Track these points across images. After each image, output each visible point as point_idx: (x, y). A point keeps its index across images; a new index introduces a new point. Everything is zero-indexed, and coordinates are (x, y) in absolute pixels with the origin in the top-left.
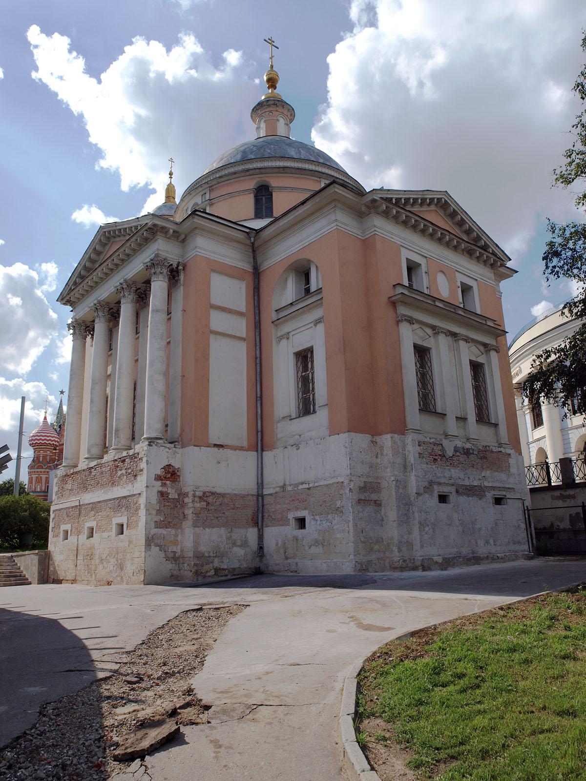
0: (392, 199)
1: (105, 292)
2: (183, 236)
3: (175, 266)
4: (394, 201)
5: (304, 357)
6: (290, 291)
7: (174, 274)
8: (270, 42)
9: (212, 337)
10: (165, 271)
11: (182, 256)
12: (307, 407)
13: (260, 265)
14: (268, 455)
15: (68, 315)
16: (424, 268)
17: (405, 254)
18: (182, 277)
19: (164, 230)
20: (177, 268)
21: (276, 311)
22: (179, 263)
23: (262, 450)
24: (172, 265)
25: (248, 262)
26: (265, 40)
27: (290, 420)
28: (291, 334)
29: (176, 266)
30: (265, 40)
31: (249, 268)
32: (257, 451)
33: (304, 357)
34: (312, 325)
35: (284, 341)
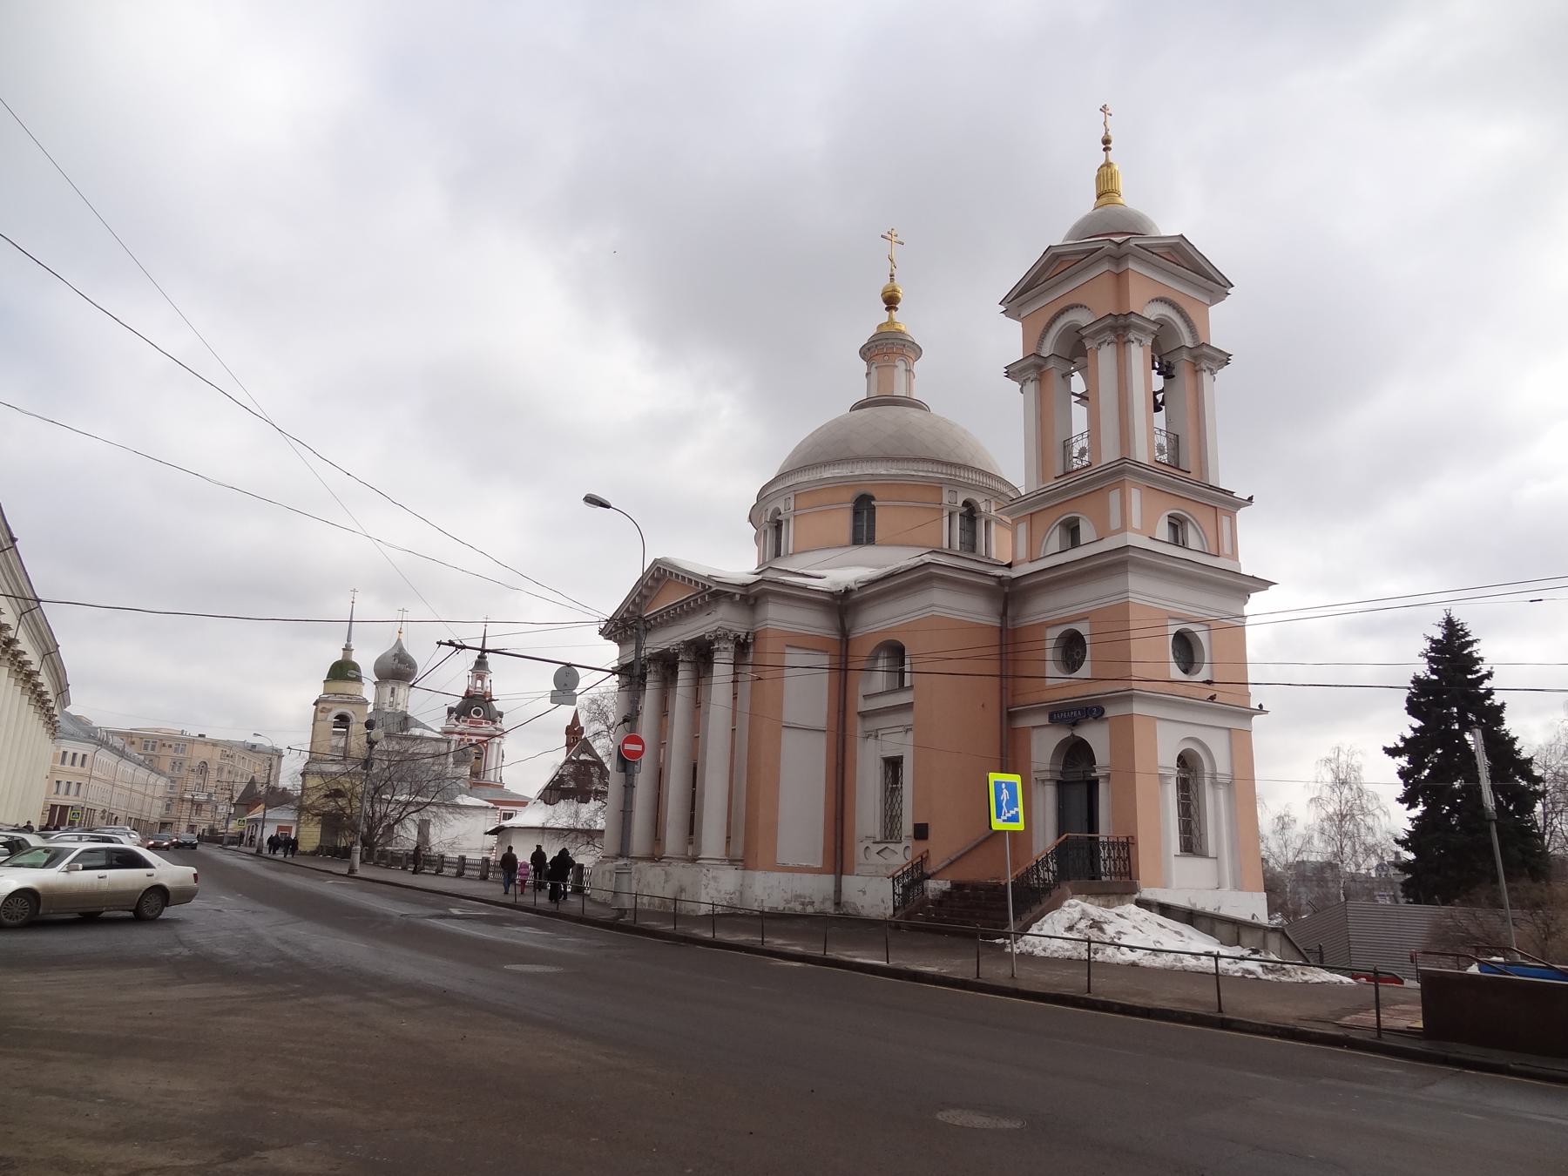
3: (743, 636)
5: (893, 765)
6: (879, 681)
7: (742, 647)
9: (785, 732)
10: (730, 646)
13: (849, 631)
19: (730, 596)
20: (745, 640)
22: (748, 634)
23: (842, 874)
24: (739, 636)
26: (882, 236)
30: (882, 236)
32: (835, 873)
33: (893, 765)
35: (871, 741)
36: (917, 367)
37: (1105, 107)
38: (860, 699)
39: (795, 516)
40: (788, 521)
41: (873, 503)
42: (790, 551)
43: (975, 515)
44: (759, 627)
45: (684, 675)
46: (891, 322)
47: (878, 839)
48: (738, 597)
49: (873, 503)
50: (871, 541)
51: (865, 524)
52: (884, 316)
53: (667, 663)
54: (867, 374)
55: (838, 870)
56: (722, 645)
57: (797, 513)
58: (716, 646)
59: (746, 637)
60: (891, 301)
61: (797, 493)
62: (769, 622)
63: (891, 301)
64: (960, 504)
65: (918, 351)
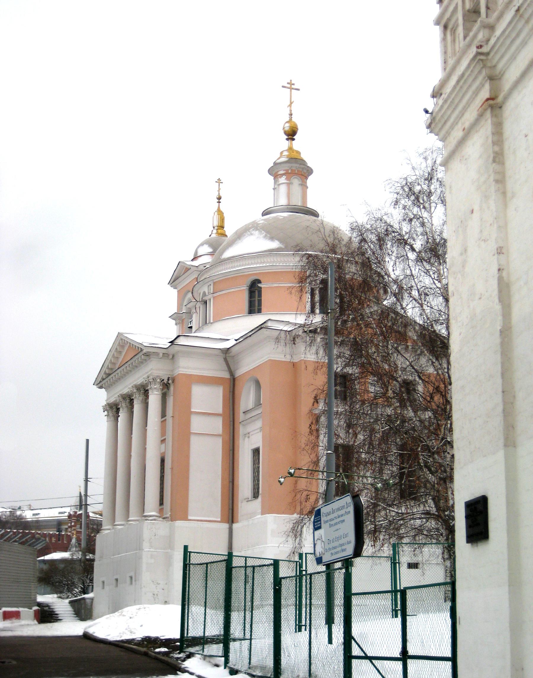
2: (171, 357)
3: (165, 381)
5: (256, 452)
7: (166, 386)
10: (157, 386)
11: (172, 371)
12: (256, 495)
14: (235, 526)
18: (172, 388)
19: (157, 354)
21: (244, 413)
22: (169, 378)
23: (233, 522)
24: (163, 380)
25: (223, 371)
26: (283, 87)
27: (247, 501)
28: (250, 434)
29: (167, 381)
30: (283, 87)
31: (227, 375)
32: (228, 523)
34: (259, 430)
35: (246, 439)
36: (310, 181)
37: (291, 83)
38: (241, 414)
39: (214, 298)
40: (210, 300)
41: (260, 285)
42: (212, 321)
44: (177, 372)
45: (137, 407)
46: (290, 149)
47: (250, 499)
48: (161, 355)
49: (260, 285)
50: (259, 311)
52: (286, 144)
53: (129, 399)
54: (274, 189)
55: (230, 521)
56: (153, 386)
57: (215, 295)
59: (168, 380)
60: (291, 134)
61: (215, 281)
62: (180, 369)
63: (291, 134)
65: (310, 171)
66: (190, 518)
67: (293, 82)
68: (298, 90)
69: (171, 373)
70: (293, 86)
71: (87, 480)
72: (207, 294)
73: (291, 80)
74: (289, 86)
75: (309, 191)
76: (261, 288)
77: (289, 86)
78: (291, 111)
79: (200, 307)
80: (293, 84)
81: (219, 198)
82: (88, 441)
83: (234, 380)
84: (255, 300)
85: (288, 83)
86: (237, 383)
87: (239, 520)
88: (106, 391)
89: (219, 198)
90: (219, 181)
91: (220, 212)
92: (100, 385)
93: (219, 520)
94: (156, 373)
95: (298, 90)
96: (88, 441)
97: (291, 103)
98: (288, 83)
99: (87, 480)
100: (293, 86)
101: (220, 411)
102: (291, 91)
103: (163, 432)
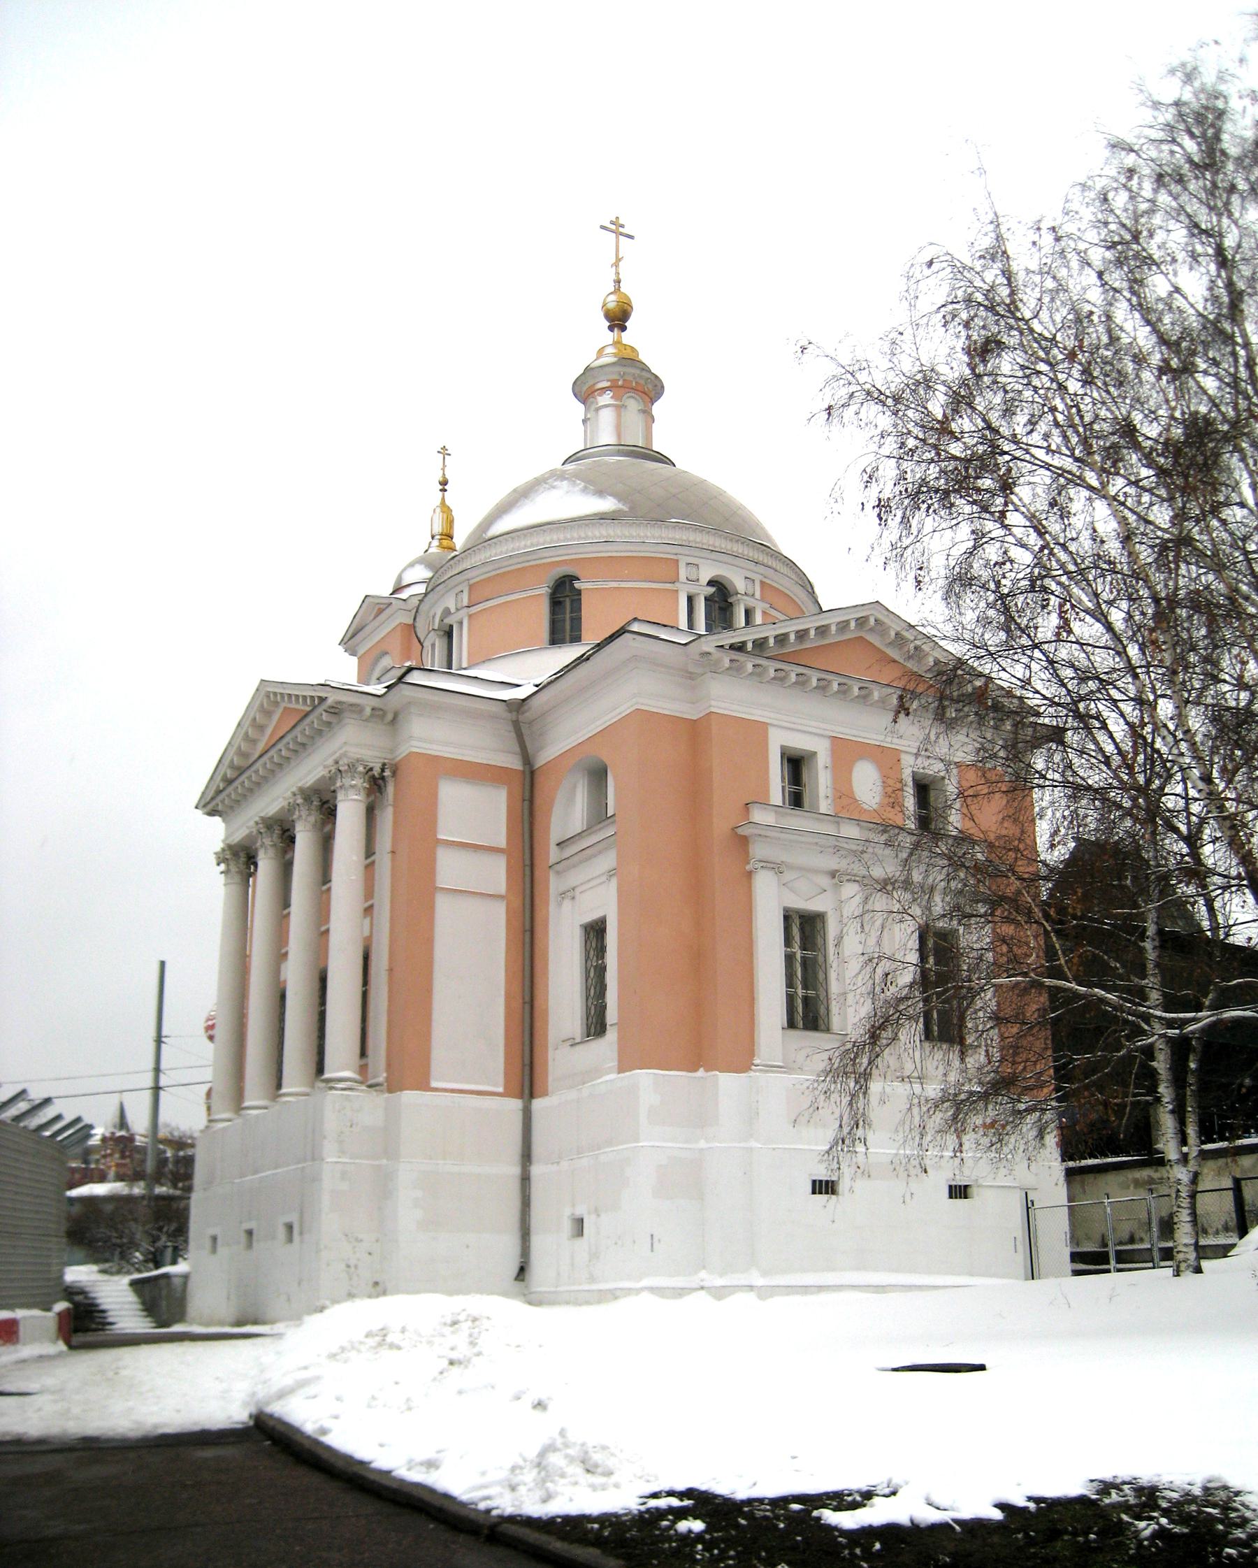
0: (744, 643)
1: (272, 801)
2: (390, 717)
3: (376, 772)
4: (750, 646)
5: (595, 932)
7: (376, 784)
8: (616, 228)
10: (358, 781)
11: (392, 751)
12: (596, 1025)
14: (537, 1104)
15: (215, 833)
16: (823, 759)
17: (778, 740)
18: (390, 789)
19: (357, 709)
22: (384, 764)
23: (532, 1096)
24: (371, 769)
25: (509, 752)
26: (603, 227)
27: (572, 1045)
28: (578, 890)
30: (603, 227)
31: (515, 763)
32: (521, 1096)
34: (604, 878)
35: (567, 904)
36: (657, 409)
38: (553, 849)
39: (470, 616)
40: (461, 623)
43: (730, 600)
45: (304, 841)
47: (578, 1040)
48: (368, 711)
51: (568, 616)
52: (609, 337)
54: (584, 421)
55: (527, 1091)
56: (348, 781)
57: (473, 610)
58: (338, 784)
59: (383, 770)
60: (618, 318)
61: (472, 582)
62: (414, 743)
63: (618, 318)
64: (705, 579)
66: (434, 1084)
67: (621, 222)
68: (631, 237)
69: (389, 756)
70: (621, 230)
71: (159, 1041)
72: (453, 610)
73: (617, 218)
74: (613, 227)
75: (656, 427)
76: (579, 592)
77: (613, 227)
78: (617, 273)
79: (433, 645)
80: (622, 226)
81: (444, 483)
82: (163, 964)
83: (532, 773)
84: (564, 620)
85: (612, 223)
86: (539, 780)
87: (550, 1088)
88: (224, 821)
89: (444, 483)
90: (444, 452)
91: (445, 508)
92: (210, 807)
93: (501, 1090)
94: (355, 752)
95: (631, 237)
96: (163, 964)
97: (618, 260)
98: (612, 223)
99: (159, 1041)
100: (621, 230)
101: (502, 842)
102: (617, 238)
103: (369, 889)
